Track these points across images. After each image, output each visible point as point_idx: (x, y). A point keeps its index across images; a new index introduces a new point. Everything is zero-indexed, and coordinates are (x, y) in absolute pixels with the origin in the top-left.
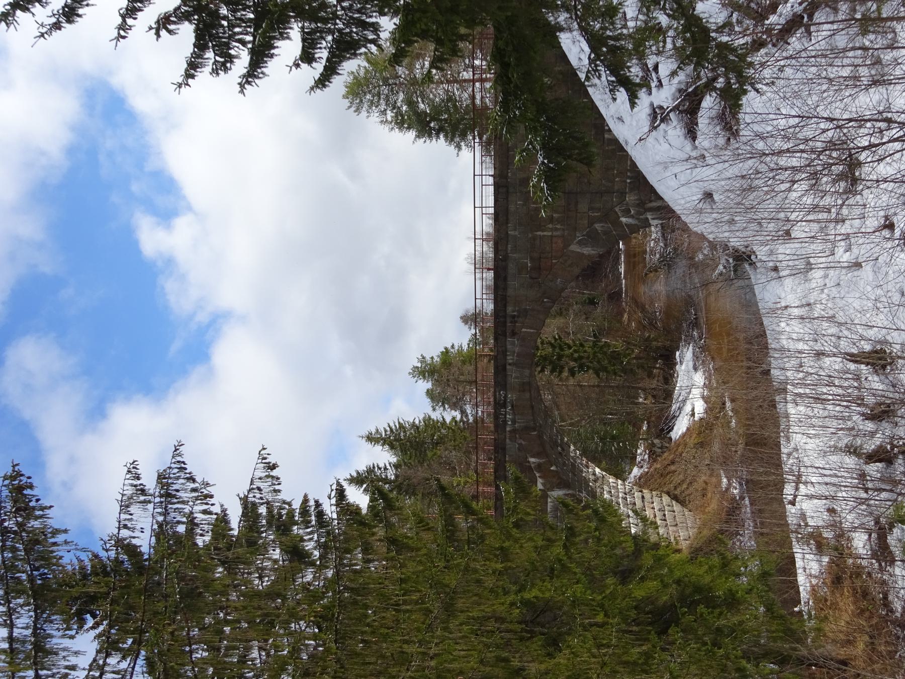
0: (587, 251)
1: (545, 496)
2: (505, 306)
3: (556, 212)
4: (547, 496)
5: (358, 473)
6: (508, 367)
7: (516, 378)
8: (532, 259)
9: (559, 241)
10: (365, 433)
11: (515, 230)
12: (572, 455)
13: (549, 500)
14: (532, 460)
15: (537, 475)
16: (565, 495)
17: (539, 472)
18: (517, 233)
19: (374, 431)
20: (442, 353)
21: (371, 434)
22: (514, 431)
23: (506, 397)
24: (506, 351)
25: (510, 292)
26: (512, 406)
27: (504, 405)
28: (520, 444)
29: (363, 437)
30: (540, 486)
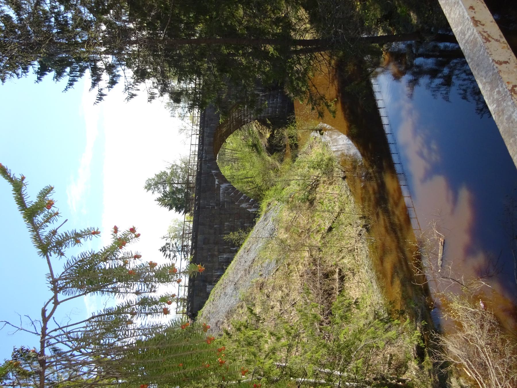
1: (219, 187)
4: (220, 187)
7: (208, 141)
13: (221, 188)
14: (213, 171)
15: (215, 177)
16: (229, 186)
17: (216, 176)
23: (203, 147)
25: (207, 113)
26: (205, 152)
28: (208, 166)
30: (217, 183)
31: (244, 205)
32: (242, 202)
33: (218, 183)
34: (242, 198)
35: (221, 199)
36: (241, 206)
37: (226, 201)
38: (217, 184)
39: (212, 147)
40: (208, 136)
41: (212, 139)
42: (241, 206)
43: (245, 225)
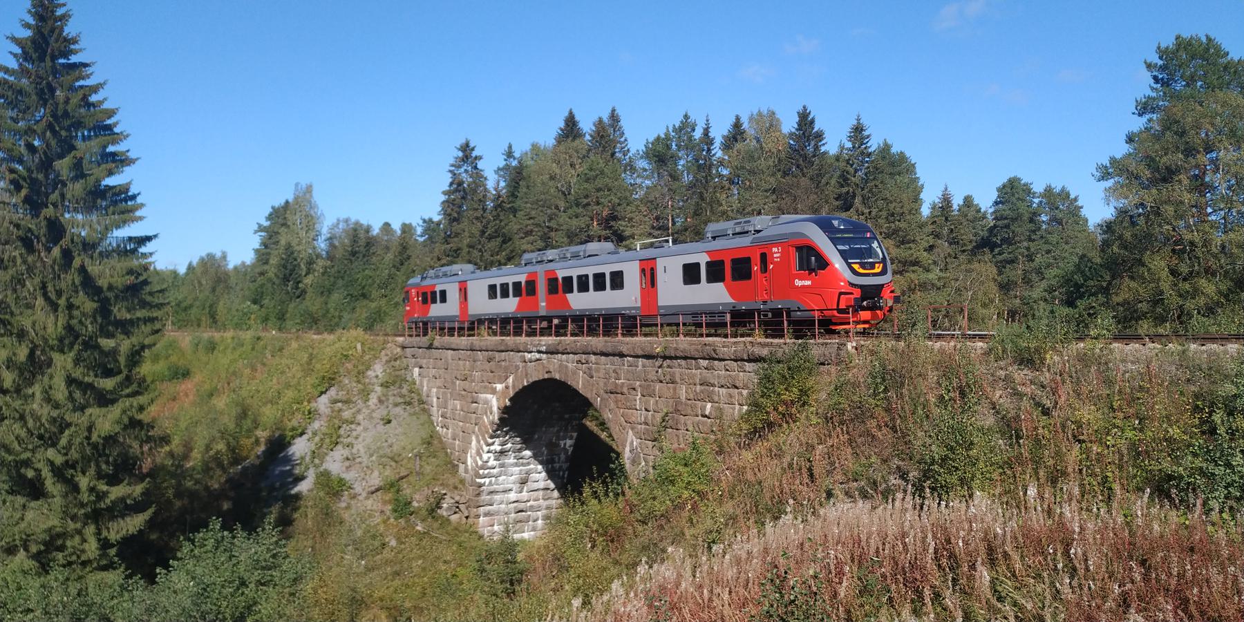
0: (627, 449)
1: (494, 391)
2: (595, 354)
3: (652, 415)
5: (812, 122)
6: (560, 355)
8: (623, 383)
9: (634, 419)
10: (864, 121)
11: (644, 366)
12: (567, 416)
14: (510, 380)
15: (504, 385)
18: (640, 368)
19: (866, 133)
20: (1068, 195)
21: (862, 130)
22: (525, 362)
24: (568, 353)
27: (539, 352)
29: (858, 120)
30: (499, 387)
31: (474, 443)
32: (478, 442)
33: (498, 389)
34: (482, 442)
35: (482, 395)
36: (474, 438)
37: (477, 408)
38: (496, 388)
39: (546, 376)
40: (560, 366)
41: (557, 377)
42: (474, 438)
43: (457, 442)
